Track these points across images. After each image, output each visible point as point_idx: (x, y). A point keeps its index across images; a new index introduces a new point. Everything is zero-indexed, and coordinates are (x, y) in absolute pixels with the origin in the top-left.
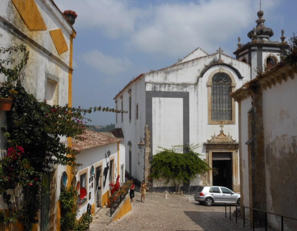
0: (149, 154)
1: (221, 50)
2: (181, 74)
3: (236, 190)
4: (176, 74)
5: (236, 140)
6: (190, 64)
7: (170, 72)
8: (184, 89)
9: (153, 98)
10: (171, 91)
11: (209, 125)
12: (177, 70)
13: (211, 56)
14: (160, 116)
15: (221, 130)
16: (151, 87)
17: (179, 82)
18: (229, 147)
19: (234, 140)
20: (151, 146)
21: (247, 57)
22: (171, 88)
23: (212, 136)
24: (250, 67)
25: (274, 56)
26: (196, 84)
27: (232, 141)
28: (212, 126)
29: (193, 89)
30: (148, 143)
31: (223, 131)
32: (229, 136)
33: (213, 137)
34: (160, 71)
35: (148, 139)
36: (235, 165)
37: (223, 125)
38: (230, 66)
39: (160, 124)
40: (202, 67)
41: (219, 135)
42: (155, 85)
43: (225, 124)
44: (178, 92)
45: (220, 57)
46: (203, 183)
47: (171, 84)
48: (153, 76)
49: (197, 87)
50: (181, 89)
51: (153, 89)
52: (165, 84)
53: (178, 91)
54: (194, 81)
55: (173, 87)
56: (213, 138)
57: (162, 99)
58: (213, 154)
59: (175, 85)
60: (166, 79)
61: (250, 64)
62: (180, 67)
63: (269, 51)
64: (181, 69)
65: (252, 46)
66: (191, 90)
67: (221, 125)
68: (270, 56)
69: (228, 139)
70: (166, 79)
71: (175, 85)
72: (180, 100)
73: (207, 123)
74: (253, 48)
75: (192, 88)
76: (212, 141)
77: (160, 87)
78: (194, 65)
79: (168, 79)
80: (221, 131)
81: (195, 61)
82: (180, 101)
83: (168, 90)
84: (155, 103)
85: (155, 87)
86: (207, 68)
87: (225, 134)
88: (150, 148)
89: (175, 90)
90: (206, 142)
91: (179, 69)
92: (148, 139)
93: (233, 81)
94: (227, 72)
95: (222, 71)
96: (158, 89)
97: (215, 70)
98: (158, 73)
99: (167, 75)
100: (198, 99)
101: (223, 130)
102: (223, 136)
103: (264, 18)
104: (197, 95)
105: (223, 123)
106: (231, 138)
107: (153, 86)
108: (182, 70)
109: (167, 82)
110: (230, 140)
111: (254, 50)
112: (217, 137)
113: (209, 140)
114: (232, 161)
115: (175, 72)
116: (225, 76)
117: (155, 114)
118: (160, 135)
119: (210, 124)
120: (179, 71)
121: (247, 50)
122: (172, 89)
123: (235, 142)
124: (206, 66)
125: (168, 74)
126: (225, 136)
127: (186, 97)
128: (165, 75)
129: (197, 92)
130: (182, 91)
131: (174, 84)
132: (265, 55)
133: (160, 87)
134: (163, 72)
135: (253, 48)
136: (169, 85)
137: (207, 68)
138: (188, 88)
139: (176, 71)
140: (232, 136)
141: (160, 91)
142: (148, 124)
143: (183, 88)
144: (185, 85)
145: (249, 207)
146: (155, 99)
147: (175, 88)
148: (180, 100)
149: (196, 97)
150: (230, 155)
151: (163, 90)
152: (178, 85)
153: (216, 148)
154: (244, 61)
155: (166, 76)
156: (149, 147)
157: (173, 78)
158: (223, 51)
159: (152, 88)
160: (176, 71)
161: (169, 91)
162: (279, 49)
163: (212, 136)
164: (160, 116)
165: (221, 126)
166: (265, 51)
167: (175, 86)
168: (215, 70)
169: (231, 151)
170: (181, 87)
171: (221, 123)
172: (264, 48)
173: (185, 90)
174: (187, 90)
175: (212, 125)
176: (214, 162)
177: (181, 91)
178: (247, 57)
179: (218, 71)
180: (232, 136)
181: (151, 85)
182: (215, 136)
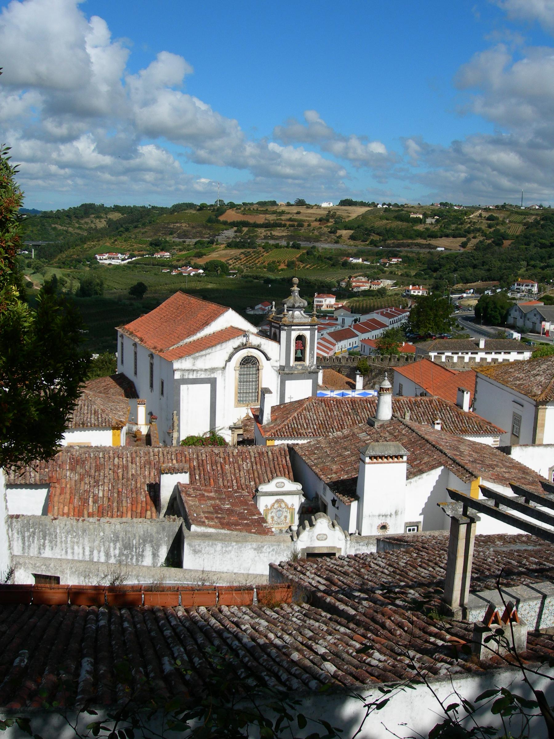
4: (204, 360)
9: (181, 386)
12: (205, 355)
17: (207, 368)
20: (179, 431)
22: (199, 375)
26: (224, 368)
29: (221, 374)
30: (176, 428)
38: (258, 348)
52: (194, 370)
54: (223, 365)
60: (194, 365)
63: (299, 330)
64: (209, 354)
70: (194, 365)
72: (208, 386)
77: (188, 374)
82: (207, 387)
85: (183, 375)
96: (186, 377)
97: (244, 353)
104: (225, 380)
109: (194, 368)
115: (204, 358)
127: (213, 382)
129: (225, 376)
130: (209, 377)
131: (201, 370)
132: (294, 334)
133: (188, 374)
136: (197, 371)
144: (213, 370)
148: (208, 386)
151: (191, 377)
152: (206, 370)
162: (309, 327)
166: (294, 330)
168: (244, 353)
170: (208, 373)
172: (293, 327)
173: (213, 376)
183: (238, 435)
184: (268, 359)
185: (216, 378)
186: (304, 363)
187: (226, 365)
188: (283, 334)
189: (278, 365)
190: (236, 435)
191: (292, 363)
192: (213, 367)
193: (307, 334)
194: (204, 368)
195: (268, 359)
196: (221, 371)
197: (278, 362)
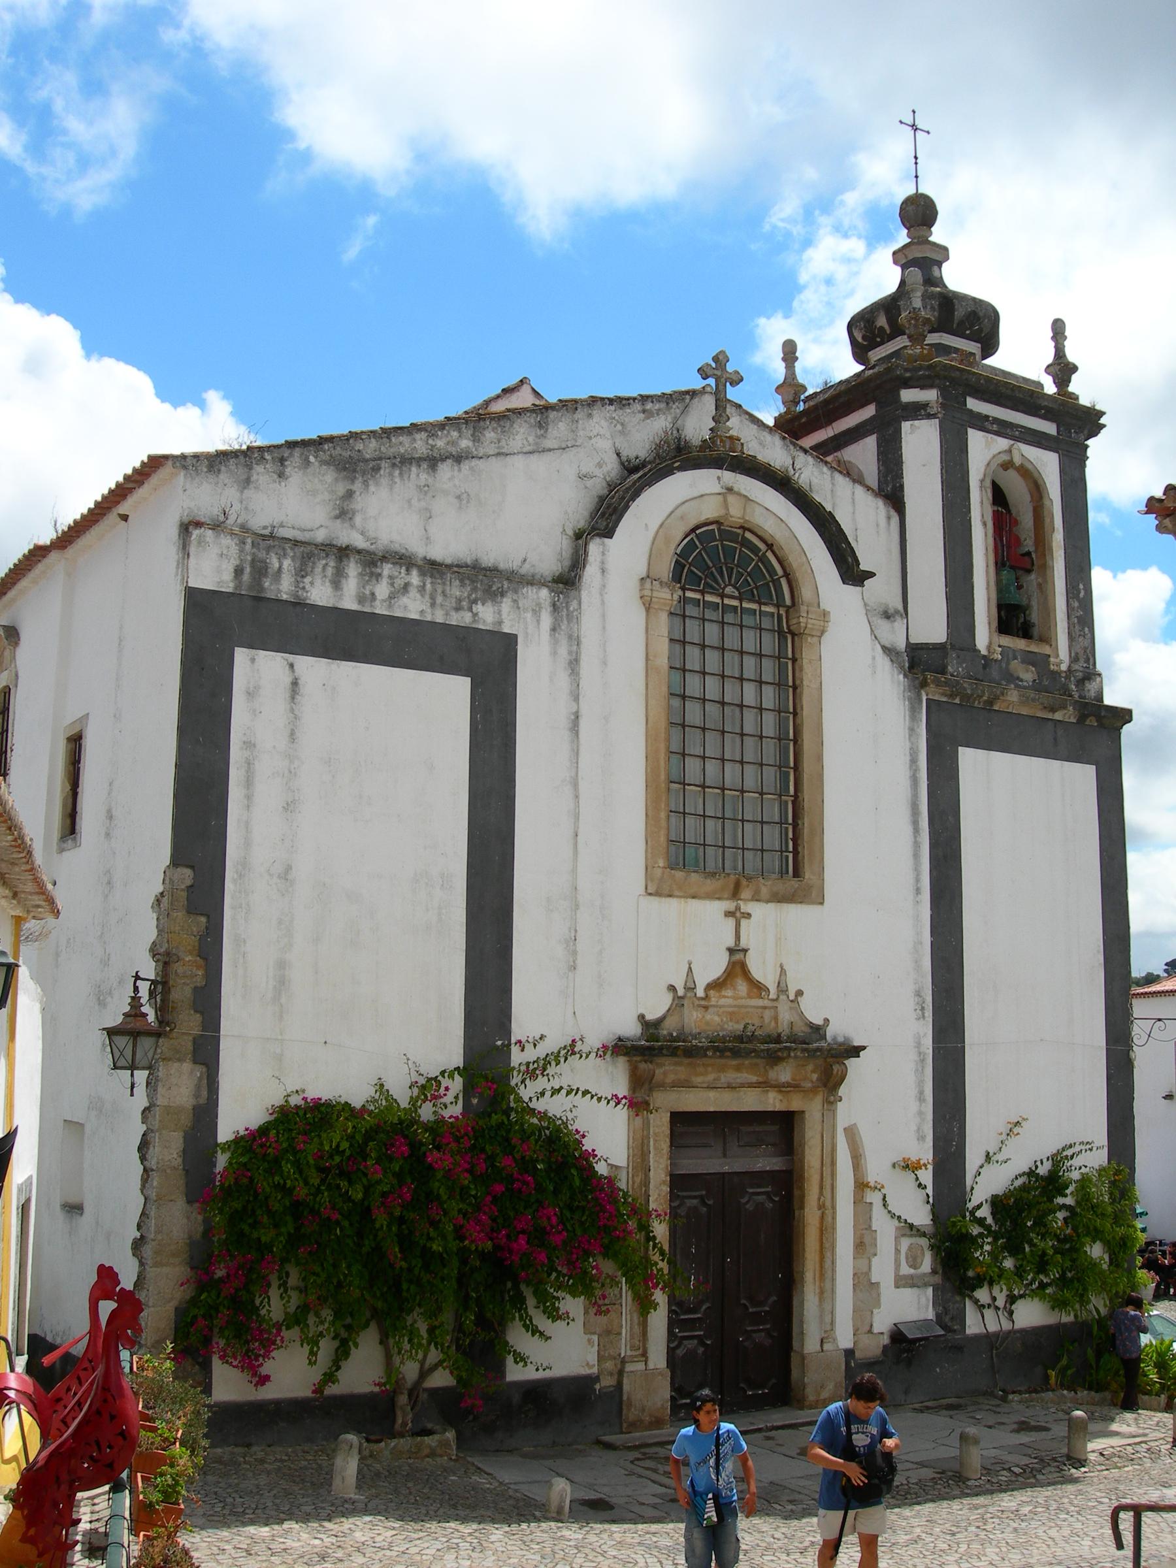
0: (186, 1120)
1: (730, 368)
2: (459, 497)
3: (825, 1394)
4: (424, 489)
5: (827, 1021)
6: (522, 434)
7: (377, 469)
8: (479, 608)
10: (380, 609)
11: (655, 901)
12: (432, 462)
13: (663, 405)
14: (289, 807)
15: (731, 942)
16: (235, 562)
17: (439, 552)
18: (784, 1073)
21: (864, 454)
22: (382, 590)
23: (672, 988)
24: (895, 519)
25: (1030, 467)
26: (567, 581)
27: (800, 1029)
28: (672, 907)
29: (546, 619)
30: (189, 1024)
31: (745, 951)
32: (782, 989)
33: (681, 992)
34: (297, 452)
35: (188, 991)
36: (821, 1207)
37: (746, 907)
39: (286, 874)
40: (599, 465)
41: (716, 985)
42: (262, 554)
43: (756, 898)
44: (433, 624)
45: (720, 415)
46: (600, 1358)
47: (384, 559)
48: (248, 481)
49: (574, 605)
50: (458, 609)
51: (246, 577)
52: (344, 553)
53: (439, 618)
54: (548, 557)
55: (399, 582)
56: (678, 1003)
57: (314, 670)
58: (679, 1119)
59: (415, 572)
60: (344, 514)
61: (893, 495)
62: (453, 443)
63: (1003, 429)
64: (459, 459)
65: (907, 384)
66: (526, 620)
67: (729, 905)
68: (1007, 466)
69: (776, 1018)
70: (344, 514)
71: (415, 572)
72: (453, 692)
73: (642, 890)
74: (908, 395)
75: (536, 612)
76: (670, 1027)
77: (301, 572)
78: (549, 443)
79: (358, 520)
80: (731, 951)
81: (552, 415)
82: (450, 696)
83: (361, 599)
84: (251, 694)
85: (260, 570)
86: (637, 476)
87: (757, 973)
88: (199, 1071)
89: (413, 607)
90: (631, 1029)
91: (443, 459)
92: (181, 993)
93: (806, 593)
94: (769, 527)
95: (736, 512)
96: (285, 588)
97: (686, 495)
98: (282, 460)
99: (357, 486)
100: (576, 699)
101: (743, 943)
102: (742, 987)
103: (938, 234)
104: (574, 664)
105: (746, 894)
107: (242, 551)
108: (466, 466)
110: (786, 1016)
111: (917, 411)
112: (707, 997)
113: (650, 1017)
114: (802, 1178)
115: (418, 475)
116: (755, 549)
117: (249, 783)
118: (281, 965)
119: (657, 894)
120: (445, 469)
121: (869, 411)
122: (392, 597)
123: (824, 1037)
124: (629, 467)
125: (366, 484)
126: (757, 988)
127: (490, 670)
128: (341, 489)
129: (575, 641)
130: (462, 619)
131: (404, 560)
133: (301, 572)
134: (323, 463)
135: (908, 395)
136: (372, 560)
137: (637, 476)
138: (506, 604)
139: (425, 465)
140: (799, 993)
141: (299, 605)
142: (192, 867)
143: (475, 602)
144: (485, 579)
145: (843, 1512)
146: (253, 660)
147: (413, 592)
148: (453, 692)
149: (563, 680)
150: (784, 1128)
151: (319, 593)
152: (433, 568)
153: (698, 1080)
154: (848, 471)
155: (350, 494)
156: (187, 1066)
157: (390, 514)
158: (742, 380)
159: (238, 571)
160: (425, 465)
161: (367, 609)
162: (1050, 428)
163: (672, 988)
164: (289, 807)
165: (729, 914)
166: (982, 423)
167: (415, 578)
169: (795, 1104)
170: (456, 591)
171: (735, 894)
172: (973, 404)
173: (486, 615)
174: (500, 623)
175: (674, 902)
176: (678, 1182)
177: (455, 619)
178: (864, 454)
179: (709, 511)
180: (799, 993)
181: (227, 541)
182: (690, 988)
183: (679, 1119)
184: (852, 572)
185: (510, 641)
186: (1046, 650)
187: (578, 563)
188: (921, 442)
189: (902, 645)
190: (660, 1124)
191: (983, 635)
192: (488, 560)
193: (1047, 464)
194: (419, 549)
195: (852, 572)
196: (544, 593)
197: (900, 625)
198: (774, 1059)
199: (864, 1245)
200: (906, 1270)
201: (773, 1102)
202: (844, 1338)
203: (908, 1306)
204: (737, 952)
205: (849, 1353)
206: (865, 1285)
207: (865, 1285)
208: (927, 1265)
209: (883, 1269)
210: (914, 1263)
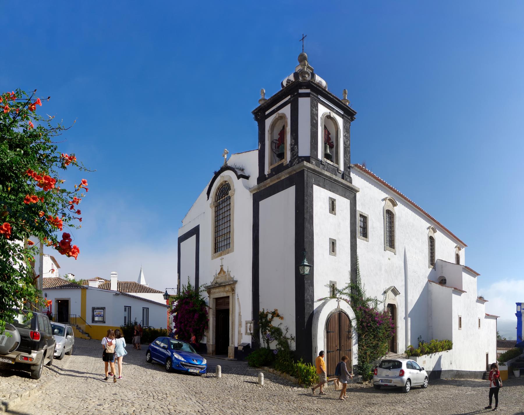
19: (232, 277)
37: (223, 257)
41: (219, 274)
106: (229, 275)
126: (224, 272)
198: (225, 286)
199: (240, 325)
200: (249, 331)
201: (225, 295)
202: (236, 346)
203: (247, 340)
204: (222, 266)
205: (236, 348)
206: (240, 334)
207: (240, 334)
208: (252, 332)
209: (243, 330)
210: (250, 330)
